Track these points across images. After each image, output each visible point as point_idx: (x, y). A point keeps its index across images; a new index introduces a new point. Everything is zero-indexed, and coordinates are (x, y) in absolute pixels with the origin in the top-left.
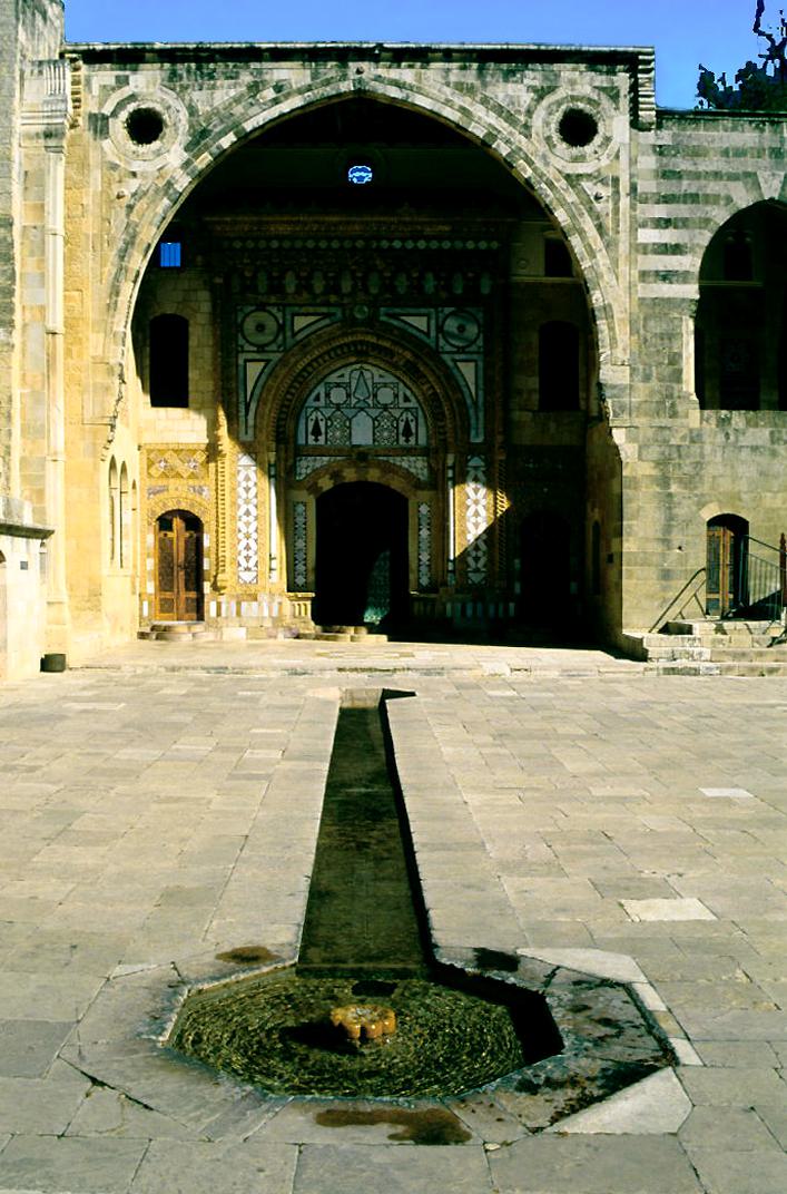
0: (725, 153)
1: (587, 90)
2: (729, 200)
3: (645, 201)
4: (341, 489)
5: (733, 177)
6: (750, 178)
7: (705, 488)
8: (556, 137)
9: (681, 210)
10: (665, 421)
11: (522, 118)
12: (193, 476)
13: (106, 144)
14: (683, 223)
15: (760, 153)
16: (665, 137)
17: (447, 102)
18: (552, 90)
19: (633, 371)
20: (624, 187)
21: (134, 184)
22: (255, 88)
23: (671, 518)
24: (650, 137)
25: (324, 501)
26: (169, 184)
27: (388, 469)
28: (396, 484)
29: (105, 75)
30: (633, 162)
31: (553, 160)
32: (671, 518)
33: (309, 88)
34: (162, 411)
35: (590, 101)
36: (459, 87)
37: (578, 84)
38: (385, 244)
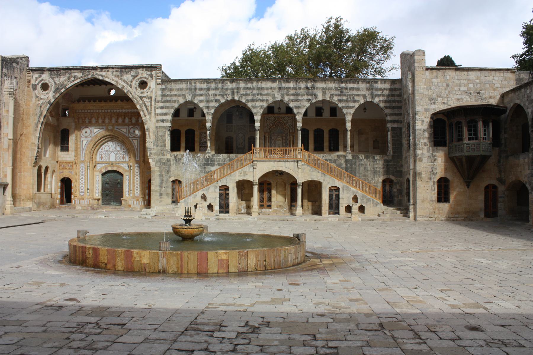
0: (178, 90)
1: (145, 75)
2: (178, 101)
3: (158, 102)
4: (108, 172)
5: (180, 96)
6: (184, 96)
7: (171, 173)
8: (138, 87)
9: (167, 104)
10: (162, 157)
11: (130, 83)
12: (69, 169)
13: (36, 91)
14: (167, 108)
15: (186, 89)
16: (164, 87)
17: (113, 80)
18: (137, 76)
19: (154, 144)
20: (153, 99)
21: (41, 101)
22: (69, 78)
23: (162, 181)
24: (160, 87)
25: (103, 174)
26: (50, 101)
27: (118, 167)
28: (121, 171)
29: (36, 75)
30: (156, 93)
31: (136, 93)
32: (162, 181)
33: (82, 77)
34: (63, 153)
35: (146, 78)
36: (116, 76)
37: (143, 74)
38: (115, 111)
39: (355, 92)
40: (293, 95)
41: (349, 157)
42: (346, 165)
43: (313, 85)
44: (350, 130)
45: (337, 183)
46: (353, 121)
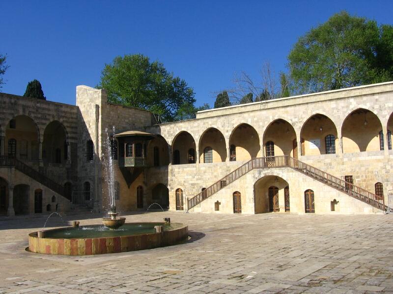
39: (47, 112)
41: (42, 164)
44: (43, 143)
46: (45, 135)
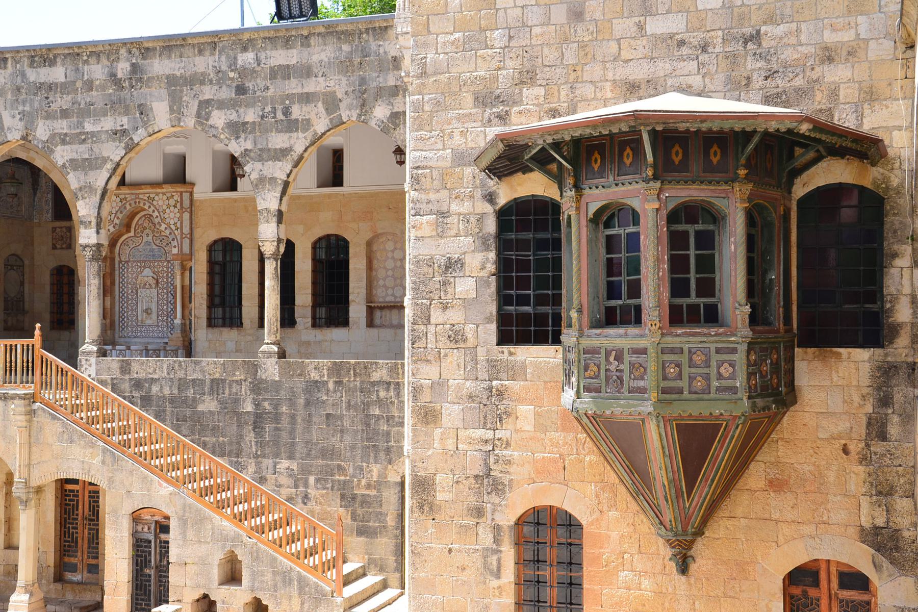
39: (294, 86)
40: (65, 114)
42: (257, 405)
43: (135, 68)
45: (162, 496)
